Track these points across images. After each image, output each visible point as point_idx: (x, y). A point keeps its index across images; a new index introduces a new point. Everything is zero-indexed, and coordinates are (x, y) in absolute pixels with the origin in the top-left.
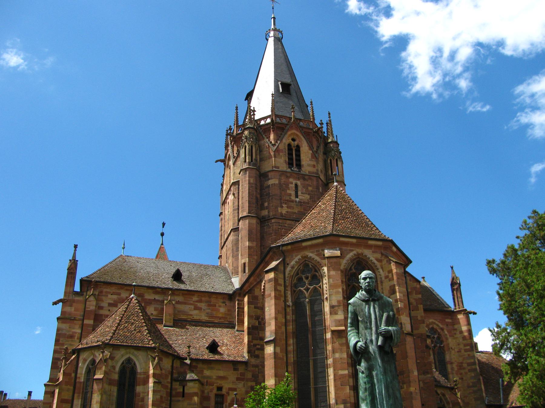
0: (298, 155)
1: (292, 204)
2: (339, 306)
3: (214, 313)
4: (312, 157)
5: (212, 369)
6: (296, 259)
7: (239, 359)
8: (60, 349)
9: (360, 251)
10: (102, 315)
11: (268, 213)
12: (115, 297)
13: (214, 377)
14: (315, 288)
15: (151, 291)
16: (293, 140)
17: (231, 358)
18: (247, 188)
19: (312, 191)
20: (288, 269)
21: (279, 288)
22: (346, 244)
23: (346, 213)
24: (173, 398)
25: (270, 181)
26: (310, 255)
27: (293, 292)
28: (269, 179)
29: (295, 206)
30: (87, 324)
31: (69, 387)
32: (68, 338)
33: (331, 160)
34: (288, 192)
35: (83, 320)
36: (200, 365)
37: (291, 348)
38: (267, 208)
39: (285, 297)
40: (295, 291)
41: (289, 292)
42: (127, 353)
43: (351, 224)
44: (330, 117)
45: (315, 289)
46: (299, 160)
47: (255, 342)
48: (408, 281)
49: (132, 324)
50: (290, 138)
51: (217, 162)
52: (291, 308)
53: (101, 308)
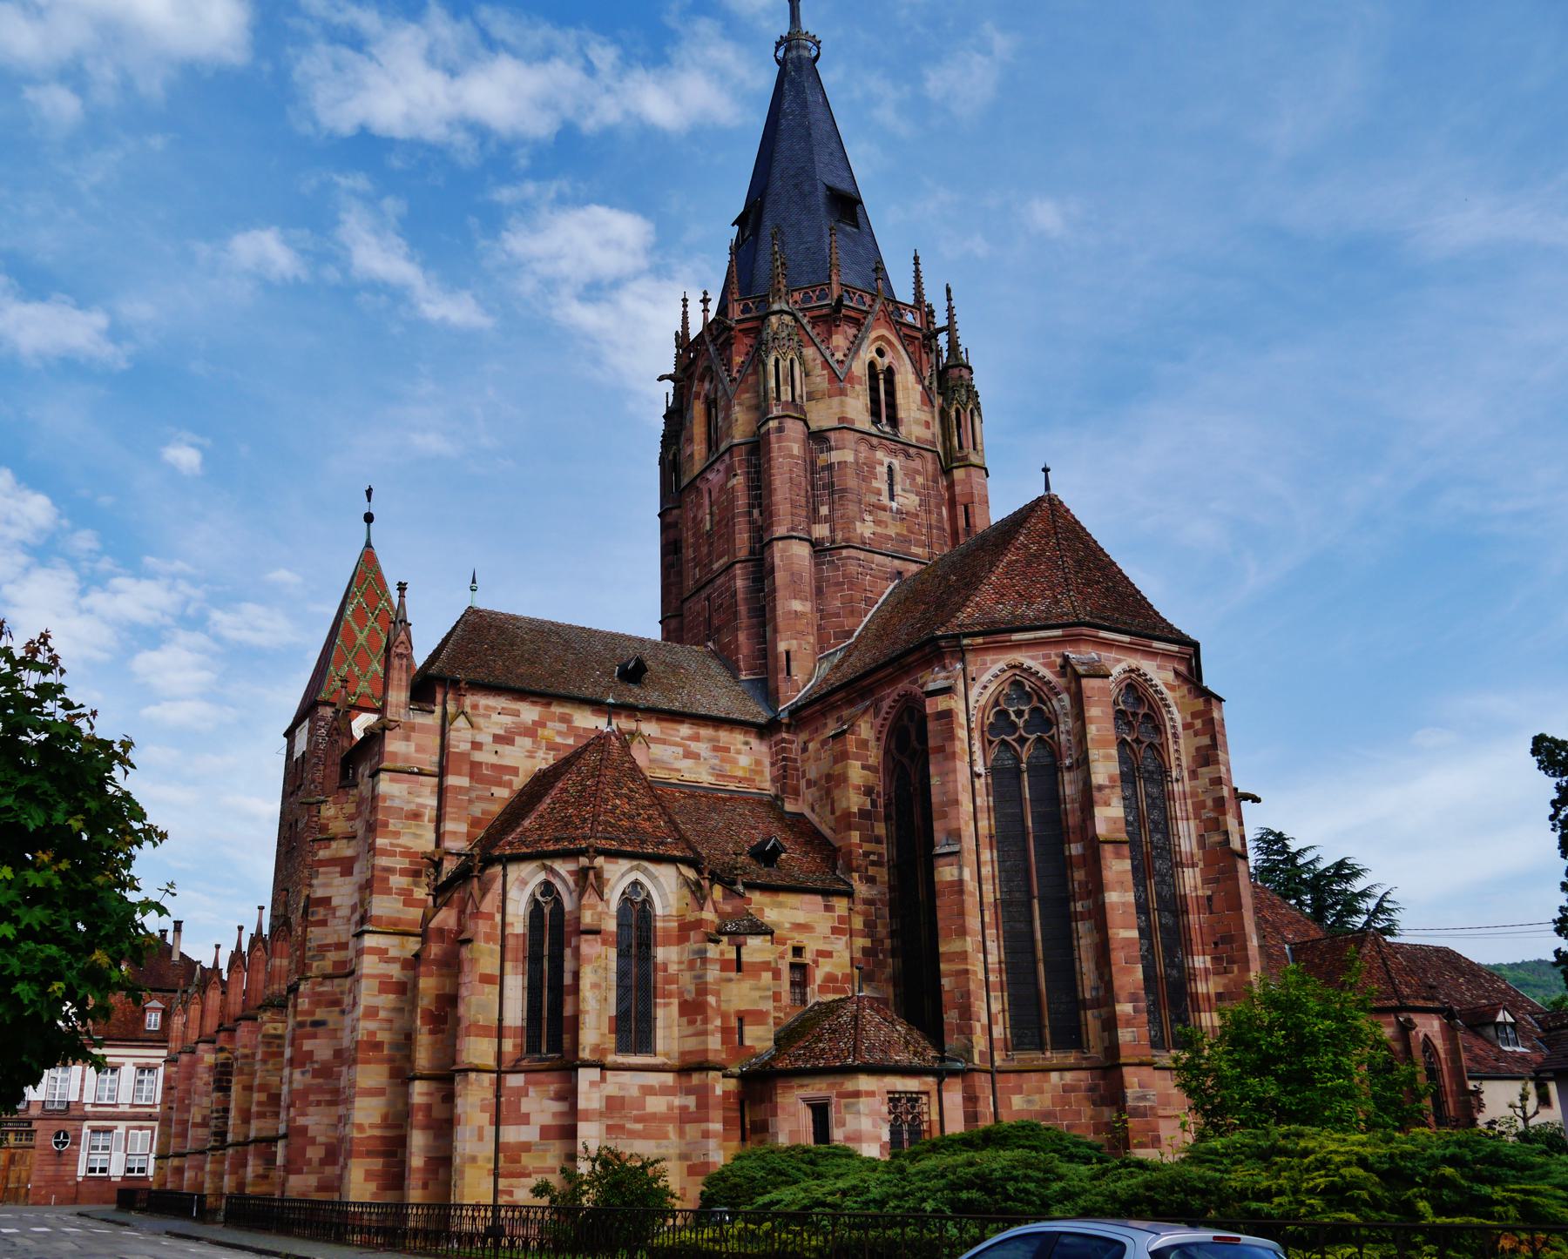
0: (891, 393)
3: (727, 767)
4: (923, 403)
5: (780, 905)
6: (995, 669)
8: (392, 845)
10: (480, 764)
11: (832, 530)
12: (507, 720)
13: (787, 926)
14: (1039, 739)
16: (880, 353)
18: (786, 469)
20: (974, 692)
25: (833, 453)
26: (1028, 663)
27: (987, 744)
28: (830, 449)
29: (890, 521)
30: (455, 787)
31: (491, 945)
32: (407, 818)
33: (957, 411)
34: (875, 484)
35: (442, 773)
37: (986, 871)
38: (827, 519)
39: (971, 753)
40: (991, 742)
42: (631, 869)
44: (949, 299)
46: (892, 406)
50: (874, 348)
51: (661, 379)
52: (983, 780)
53: (477, 746)
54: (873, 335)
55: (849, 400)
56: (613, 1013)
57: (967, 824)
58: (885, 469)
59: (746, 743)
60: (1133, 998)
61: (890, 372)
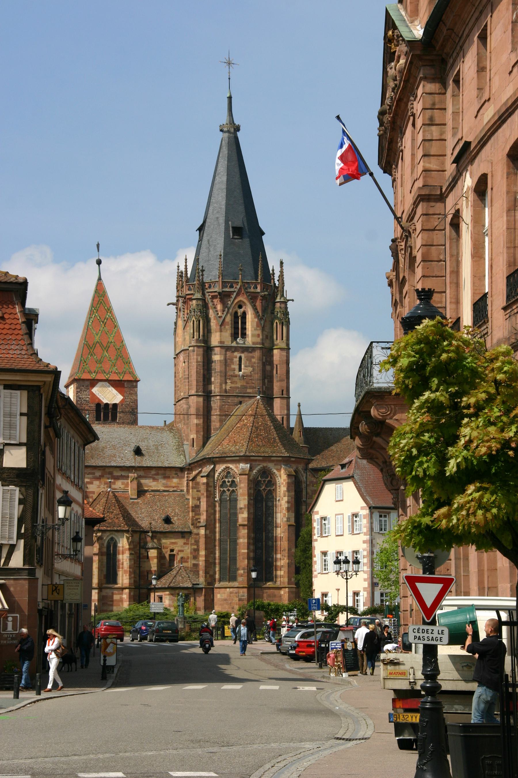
0: (244, 323)
1: (235, 379)
2: (245, 508)
3: (169, 483)
4: (257, 326)
7: (186, 530)
9: (265, 465)
15: (118, 469)
17: (180, 530)
19: (255, 363)
21: (209, 489)
22: (256, 461)
23: (260, 430)
24: (141, 560)
28: (215, 354)
29: (238, 381)
34: (233, 366)
36: (158, 535)
41: (217, 491)
43: (262, 441)
45: (233, 490)
46: (244, 329)
47: (197, 517)
48: (308, 477)
49: (112, 513)
50: (237, 306)
51: (168, 305)
54: (236, 301)
55: (222, 333)
56: (105, 573)
57: (210, 517)
58: (238, 359)
59: (176, 474)
60: (244, 569)
61: (244, 314)
